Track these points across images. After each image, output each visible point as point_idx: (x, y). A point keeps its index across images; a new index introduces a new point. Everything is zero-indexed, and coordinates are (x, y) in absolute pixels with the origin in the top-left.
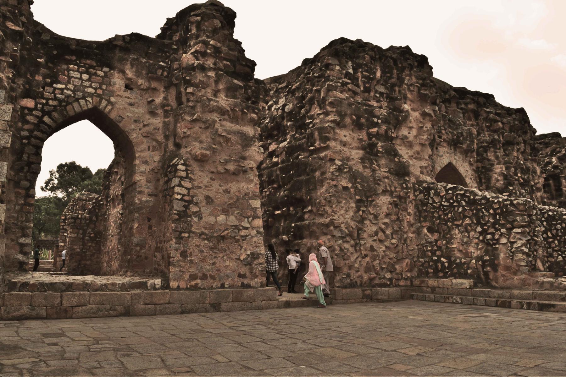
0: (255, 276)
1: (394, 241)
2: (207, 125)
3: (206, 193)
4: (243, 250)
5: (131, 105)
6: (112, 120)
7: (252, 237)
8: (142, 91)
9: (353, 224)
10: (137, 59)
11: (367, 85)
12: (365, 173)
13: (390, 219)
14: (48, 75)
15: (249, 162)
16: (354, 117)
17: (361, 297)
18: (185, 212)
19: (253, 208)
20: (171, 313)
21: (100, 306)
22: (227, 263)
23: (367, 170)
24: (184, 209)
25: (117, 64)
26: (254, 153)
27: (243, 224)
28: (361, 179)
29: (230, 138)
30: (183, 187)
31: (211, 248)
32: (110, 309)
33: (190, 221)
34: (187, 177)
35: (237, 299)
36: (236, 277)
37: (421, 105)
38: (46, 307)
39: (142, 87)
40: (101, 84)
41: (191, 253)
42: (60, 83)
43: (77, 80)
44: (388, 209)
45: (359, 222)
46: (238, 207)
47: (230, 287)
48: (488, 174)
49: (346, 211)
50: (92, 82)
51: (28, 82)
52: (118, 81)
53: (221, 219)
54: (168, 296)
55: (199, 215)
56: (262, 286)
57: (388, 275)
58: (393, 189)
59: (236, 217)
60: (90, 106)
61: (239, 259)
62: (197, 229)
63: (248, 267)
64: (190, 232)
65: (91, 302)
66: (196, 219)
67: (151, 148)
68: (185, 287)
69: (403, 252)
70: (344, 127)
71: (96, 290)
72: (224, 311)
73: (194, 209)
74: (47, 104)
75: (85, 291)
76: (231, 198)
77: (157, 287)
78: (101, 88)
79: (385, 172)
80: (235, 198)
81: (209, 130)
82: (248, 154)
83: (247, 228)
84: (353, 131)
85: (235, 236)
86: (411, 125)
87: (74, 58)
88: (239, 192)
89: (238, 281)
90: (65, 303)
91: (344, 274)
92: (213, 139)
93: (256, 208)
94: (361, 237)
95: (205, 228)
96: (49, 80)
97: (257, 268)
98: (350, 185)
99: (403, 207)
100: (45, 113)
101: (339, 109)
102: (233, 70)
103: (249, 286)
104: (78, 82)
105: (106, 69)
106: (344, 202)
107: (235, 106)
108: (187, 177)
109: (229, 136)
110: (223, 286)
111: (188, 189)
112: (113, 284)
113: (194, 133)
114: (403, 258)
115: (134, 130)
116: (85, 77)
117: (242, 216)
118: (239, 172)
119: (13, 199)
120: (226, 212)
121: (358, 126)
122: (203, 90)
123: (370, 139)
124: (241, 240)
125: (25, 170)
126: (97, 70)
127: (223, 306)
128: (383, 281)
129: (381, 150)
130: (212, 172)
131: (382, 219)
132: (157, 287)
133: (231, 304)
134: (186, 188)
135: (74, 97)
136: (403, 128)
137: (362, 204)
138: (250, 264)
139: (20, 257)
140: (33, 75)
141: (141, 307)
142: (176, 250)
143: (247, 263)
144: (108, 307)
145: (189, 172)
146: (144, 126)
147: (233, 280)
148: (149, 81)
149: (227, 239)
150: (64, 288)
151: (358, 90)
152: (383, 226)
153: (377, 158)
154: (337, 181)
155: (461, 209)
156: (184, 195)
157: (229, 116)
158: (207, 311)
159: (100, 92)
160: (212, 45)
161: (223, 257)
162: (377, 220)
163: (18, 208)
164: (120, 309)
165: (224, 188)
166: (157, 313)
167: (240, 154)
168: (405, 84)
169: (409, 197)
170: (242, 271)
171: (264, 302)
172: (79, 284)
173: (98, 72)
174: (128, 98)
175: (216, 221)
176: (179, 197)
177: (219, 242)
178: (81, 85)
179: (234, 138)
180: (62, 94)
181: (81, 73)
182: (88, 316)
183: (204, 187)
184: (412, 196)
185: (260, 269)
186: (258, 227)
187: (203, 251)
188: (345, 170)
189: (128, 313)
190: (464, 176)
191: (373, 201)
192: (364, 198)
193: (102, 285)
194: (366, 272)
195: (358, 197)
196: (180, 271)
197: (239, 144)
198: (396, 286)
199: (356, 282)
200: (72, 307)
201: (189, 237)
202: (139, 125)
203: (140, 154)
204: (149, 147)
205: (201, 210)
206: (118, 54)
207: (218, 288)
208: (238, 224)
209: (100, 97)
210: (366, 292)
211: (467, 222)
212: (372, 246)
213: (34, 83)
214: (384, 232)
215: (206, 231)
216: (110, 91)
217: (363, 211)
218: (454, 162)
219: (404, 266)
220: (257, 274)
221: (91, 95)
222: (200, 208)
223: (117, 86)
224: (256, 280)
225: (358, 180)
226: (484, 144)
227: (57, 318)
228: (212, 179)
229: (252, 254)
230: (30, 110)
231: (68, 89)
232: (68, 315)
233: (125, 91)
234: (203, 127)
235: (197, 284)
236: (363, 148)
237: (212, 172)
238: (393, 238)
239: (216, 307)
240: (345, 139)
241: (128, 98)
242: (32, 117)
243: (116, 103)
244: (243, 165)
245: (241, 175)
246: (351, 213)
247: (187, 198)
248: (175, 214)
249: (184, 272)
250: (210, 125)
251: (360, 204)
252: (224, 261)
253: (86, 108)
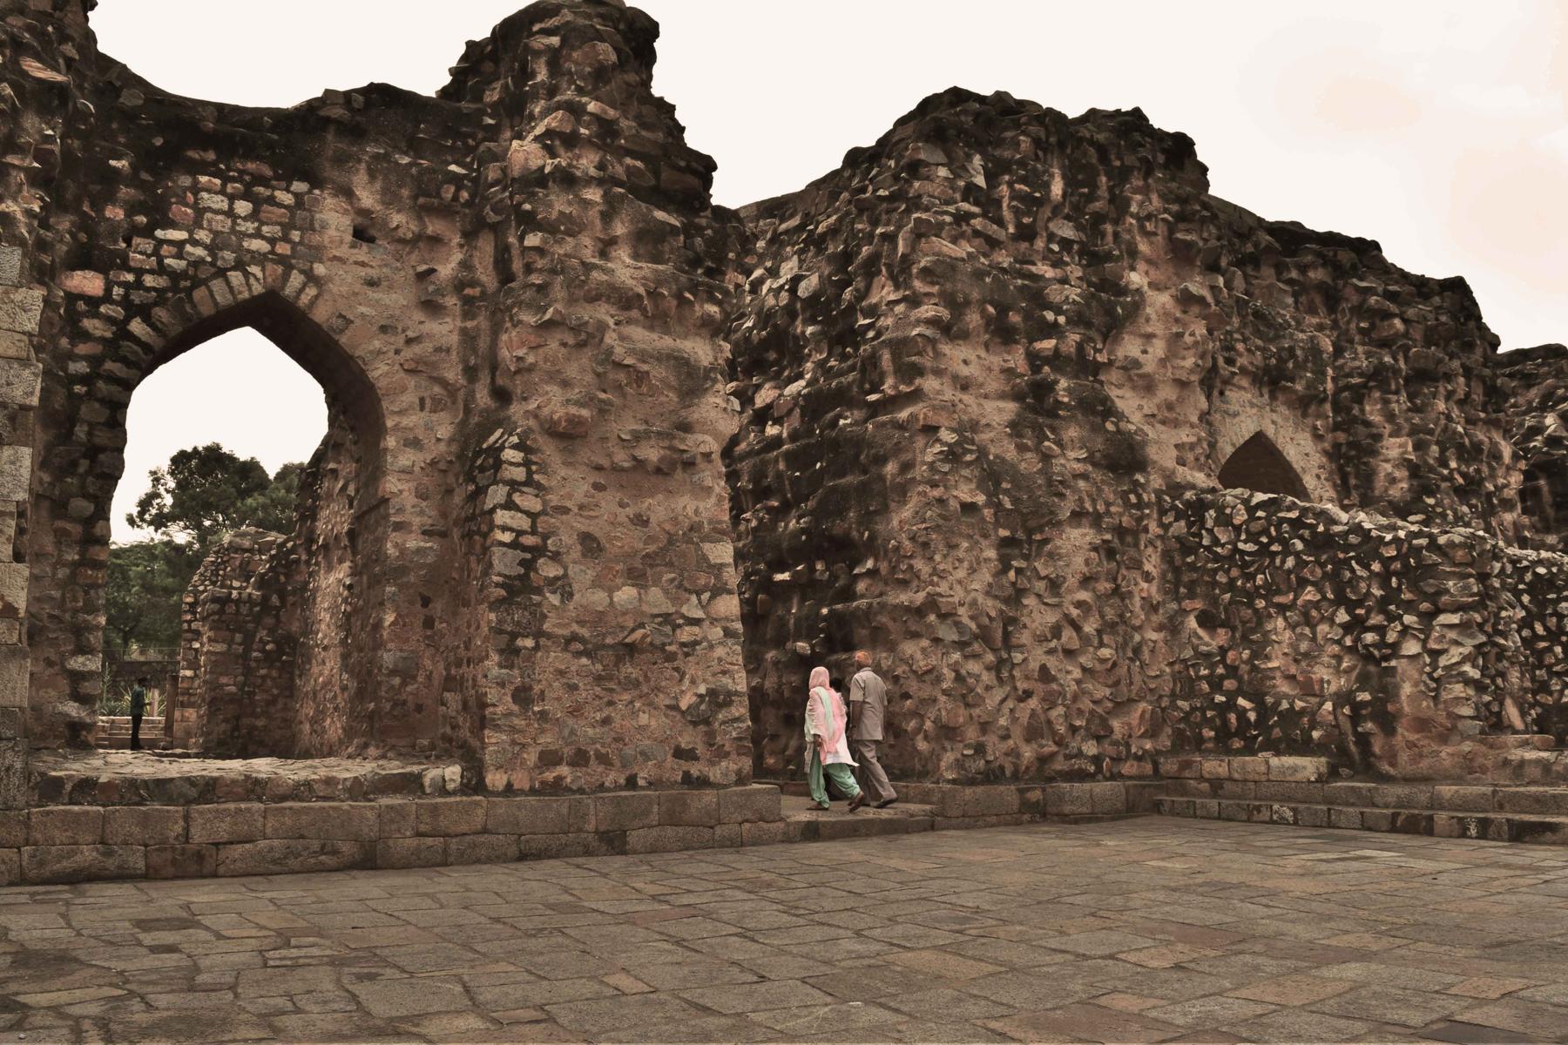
0: (722, 754)
1: (1105, 652)
2: (583, 336)
3: (582, 525)
4: (686, 682)
5: (372, 283)
6: (318, 326)
7: (711, 647)
8: (400, 247)
9: (991, 606)
10: (386, 157)
11: (1026, 220)
12: (1023, 465)
13: (1094, 590)
14: (141, 203)
15: (700, 437)
16: (991, 309)
17: (1015, 808)
18: (524, 578)
19: (714, 566)
20: (489, 860)
21: (292, 842)
22: (644, 719)
23: (1029, 455)
24: (522, 571)
26: (713, 414)
27: (684, 610)
28: (1012, 482)
29: (647, 373)
30: (518, 509)
31: (599, 679)
32: (323, 851)
33: (539, 605)
34: (529, 482)
35: (672, 819)
36: (670, 758)
37: (1177, 274)
38: (146, 846)
39: (400, 233)
40: (287, 228)
41: (542, 692)
42: (173, 225)
43: (220, 217)
44: (1087, 563)
45: (1006, 601)
46: (671, 564)
48: (1365, 464)
49: (972, 571)
50: (262, 223)
51: (85, 224)
52: (334, 218)
53: (625, 597)
54: (480, 812)
55: (563, 586)
56: (741, 780)
57: (1091, 748)
58: (1101, 508)
59: (666, 592)
60: (258, 289)
61: (676, 708)
62: (559, 625)
63: (702, 728)
64: (539, 634)
65: (269, 831)
66: (554, 599)
67: (428, 402)
68: (527, 787)
69: (1131, 683)
71: (284, 798)
72: (635, 852)
73: (548, 570)
74: (138, 284)
75: (250, 800)
76: (651, 539)
77: (451, 786)
78: (286, 238)
79: (1078, 460)
80: (664, 538)
81: (589, 352)
82: (696, 416)
83: (696, 622)
84: (987, 346)
85: (664, 644)
86: (1150, 330)
87: (211, 156)
88: (675, 520)
89: (674, 770)
90: (198, 835)
91: (967, 746)
92: (598, 375)
93: (722, 565)
94: (1014, 641)
95: (581, 623)
96: (142, 219)
97: (726, 733)
98: (981, 499)
99: (1131, 559)
100: (132, 310)
101: (948, 286)
102: (653, 182)
103: (704, 783)
105: (299, 186)
106: (965, 545)
107: (659, 282)
108: (529, 482)
109: (645, 367)
110: (631, 783)
111: (533, 516)
112: (329, 781)
113: (546, 360)
114: (1131, 701)
115: (380, 352)
116: (243, 207)
117: (685, 588)
118: (673, 465)
119: (50, 548)
120: (637, 577)
121: (1002, 334)
122: (569, 239)
123: (1036, 369)
124: (680, 656)
125: (81, 470)
126: (274, 188)
127: (634, 838)
128: (1077, 764)
129: (1066, 400)
130: (599, 468)
131: (1070, 591)
132: (451, 786)
133: (655, 832)
134: (528, 513)
135: (213, 264)
136: (1126, 337)
137: (1016, 551)
138: (707, 722)
139: (72, 709)
140: (98, 206)
141: (405, 843)
142: (502, 685)
143: (698, 720)
144: (315, 845)
145: (534, 468)
146: (409, 341)
147: (659, 766)
148: (420, 218)
149: (642, 651)
150: (193, 792)
151: (1001, 234)
152: (1075, 612)
153: (1057, 422)
154: (946, 487)
155: (1290, 562)
156: (520, 533)
157: (643, 310)
158: (588, 852)
159: (283, 249)
160: (591, 114)
161: (632, 702)
162: (1058, 595)
163: (62, 573)
164: (347, 848)
165: (630, 511)
166: (451, 859)
167: (674, 418)
168: (1132, 216)
169: (1146, 530)
170: (685, 742)
171: (747, 825)
172: (234, 782)
173: (277, 193)
174: (363, 264)
175: (612, 602)
176: (507, 537)
177: (619, 660)
178: (233, 230)
179: (658, 372)
180: (179, 256)
181: (232, 198)
182: (261, 870)
183: (576, 510)
184: (1154, 528)
185: (734, 734)
186: (727, 619)
187: (573, 688)
188: (969, 458)
189: (370, 860)
190: (1299, 470)
191: (1046, 541)
192: (1020, 535)
193: (298, 785)
194: (1028, 741)
195: (1004, 533)
196: (514, 743)
197: (671, 388)
198: (1113, 777)
199: (1002, 768)
200: (216, 844)
201: (537, 648)
202: (392, 339)
203: (397, 419)
204: (422, 400)
205: (570, 572)
206: (332, 143)
207: (618, 787)
208: (672, 610)
210: (1028, 795)
211: (1309, 597)
212: (1043, 668)
213: (103, 227)
214: (1077, 628)
215: (584, 632)
216: (310, 247)
217: (1019, 571)
218: (1270, 431)
219: (1135, 722)
220: (727, 748)
221: (260, 259)
222: (566, 569)
223: (332, 232)
224: (723, 764)
225: (1005, 485)
226: (1356, 380)
227: (175, 878)
228: (598, 487)
229: (712, 693)
230: (93, 302)
231: (196, 243)
232: (207, 869)
233: (353, 246)
234: (571, 341)
235: (560, 779)
236: (1017, 396)
237: (599, 468)
238: (1102, 645)
239: (613, 842)
240: (965, 371)
241: (363, 264)
242: (96, 322)
243: (329, 279)
244: (683, 447)
245: (679, 474)
246: (986, 575)
247: (529, 540)
248: (497, 585)
249: (524, 746)
250: (590, 336)
251: (1009, 551)
252: (634, 714)
253: (246, 295)
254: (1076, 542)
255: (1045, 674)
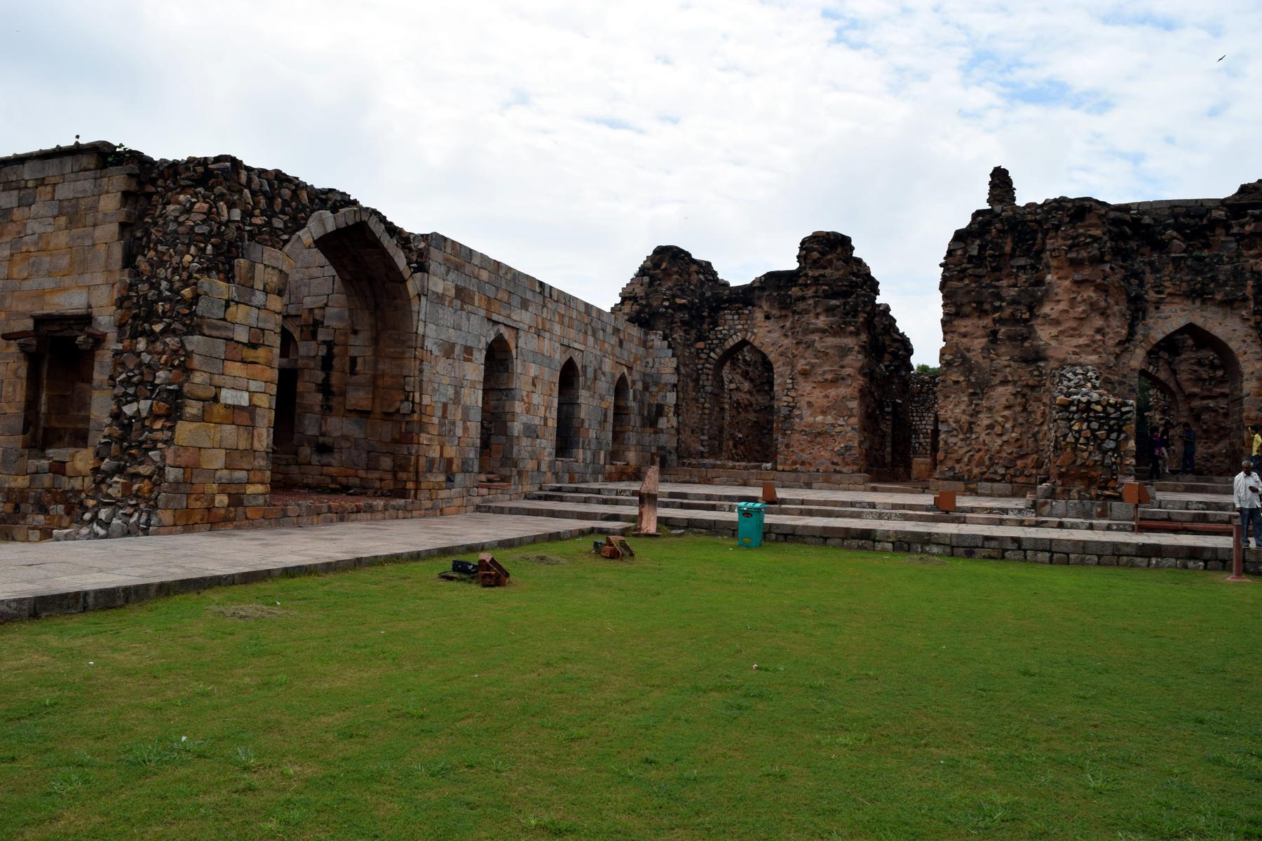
0: (847, 464)
25: (757, 302)
45: (971, 416)
47: (825, 472)
51: (699, 331)
52: (759, 315)
57: (1001, 471)
70: (967, 316)
84: (979, 317)
89: (832, 468)
98: (962, 379)
103: (840, 472)
104: (731, 323)
120: (824, 413)
121: (982, 313)
139: (701, 448)
152: (1000, 419)
192: (978, 391)
209: (747, 331)
217: (977, 405)
218: (1199, 322)
221: (740, 331)
240: (963, 330)
246: (963, 407)
254: (1002, 394)
255: (984, 444)
